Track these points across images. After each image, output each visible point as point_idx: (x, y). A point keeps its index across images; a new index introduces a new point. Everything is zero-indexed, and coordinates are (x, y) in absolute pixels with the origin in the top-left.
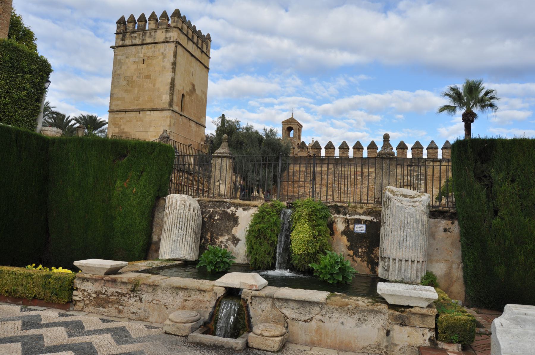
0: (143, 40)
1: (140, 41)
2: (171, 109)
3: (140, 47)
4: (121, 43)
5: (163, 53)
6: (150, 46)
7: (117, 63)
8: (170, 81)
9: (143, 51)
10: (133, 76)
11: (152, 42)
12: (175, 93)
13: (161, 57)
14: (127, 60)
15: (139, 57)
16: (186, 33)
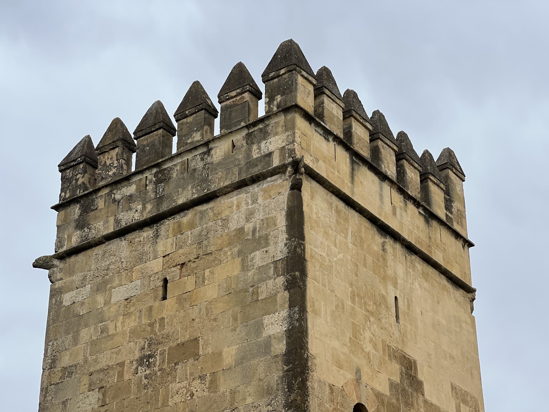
1: (149, 207)
3: (147, 233)
7: (61, 321)
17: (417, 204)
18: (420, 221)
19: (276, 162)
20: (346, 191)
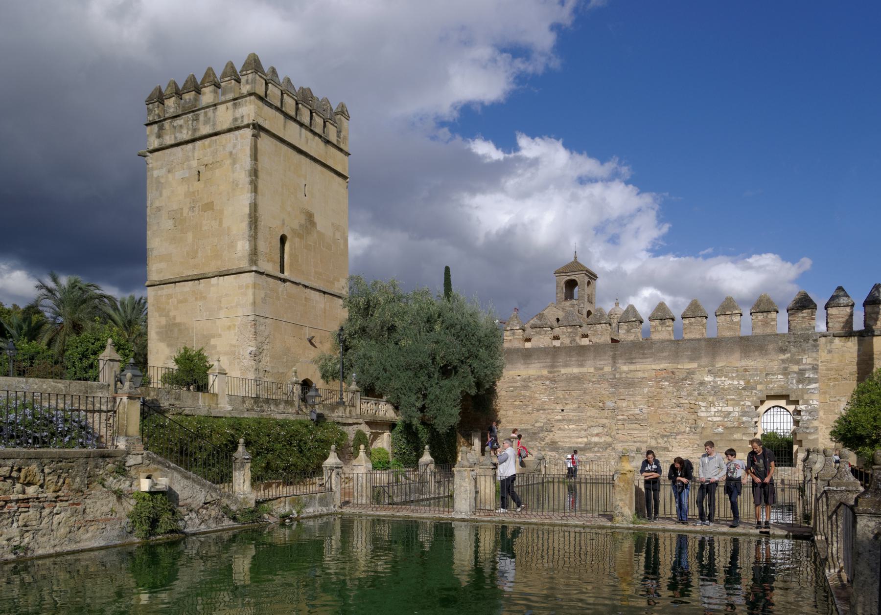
0: (195, 130)
1: (190, 133)
2: (254, 268)
3: (190, 146)
4: (155, 143)
5: (231, 153)
6: (207, 141)
8: (247, 210)
9: (196, 154)
10: (182, 209)
11: (211, 132)
12: (260, 235)
13: (228, 162)
14: (170, 176)
15: (190, 168)
16: (279, 105)
17: (320, 137)
18: (321, 144)
19: (246, 122)
20: (281, 135)
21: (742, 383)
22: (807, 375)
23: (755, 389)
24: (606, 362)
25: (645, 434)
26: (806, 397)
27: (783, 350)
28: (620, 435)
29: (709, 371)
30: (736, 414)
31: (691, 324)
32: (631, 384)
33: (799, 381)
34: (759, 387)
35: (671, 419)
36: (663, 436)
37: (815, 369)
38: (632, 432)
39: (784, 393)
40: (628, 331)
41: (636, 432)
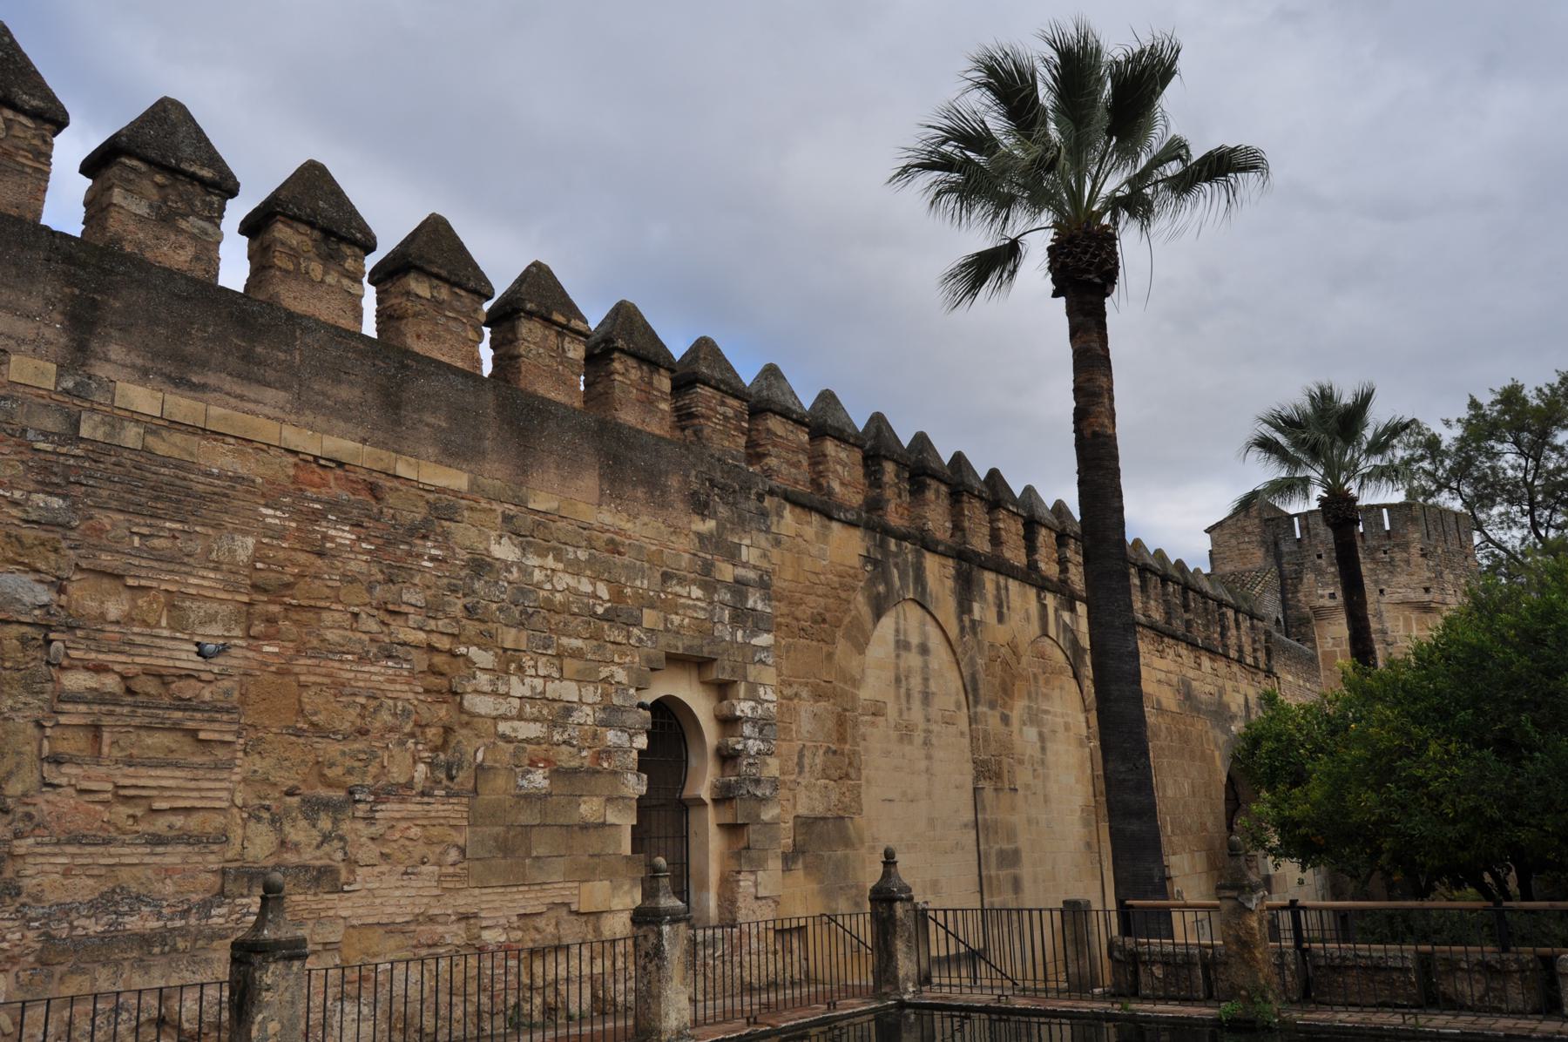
21: (603, 591)
22: (750, 604)
23: (638, 624)
24: (23, 328)
25: (221, 791)
26: (753, 672)
27: (701, 507)
28: (66, 801)
29: (507, 519)
30: (585, 716)
31: (437, 303)
32: (168, 493)
33: (741, 615)
34: (650, 618)
35: (349, 719)
36: (313, 807)
37: (764, 585)
38: (148, 778)
39: (706, 652)
40: (165, 218)
41: (168, 778)
